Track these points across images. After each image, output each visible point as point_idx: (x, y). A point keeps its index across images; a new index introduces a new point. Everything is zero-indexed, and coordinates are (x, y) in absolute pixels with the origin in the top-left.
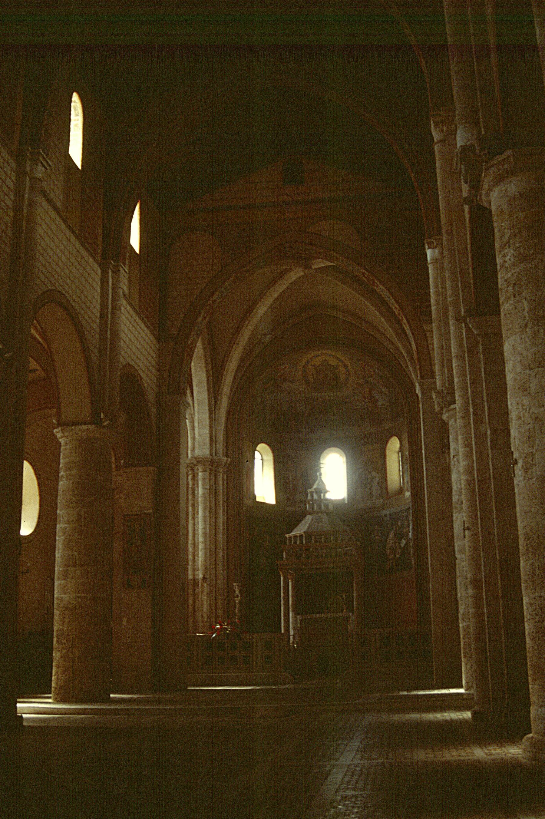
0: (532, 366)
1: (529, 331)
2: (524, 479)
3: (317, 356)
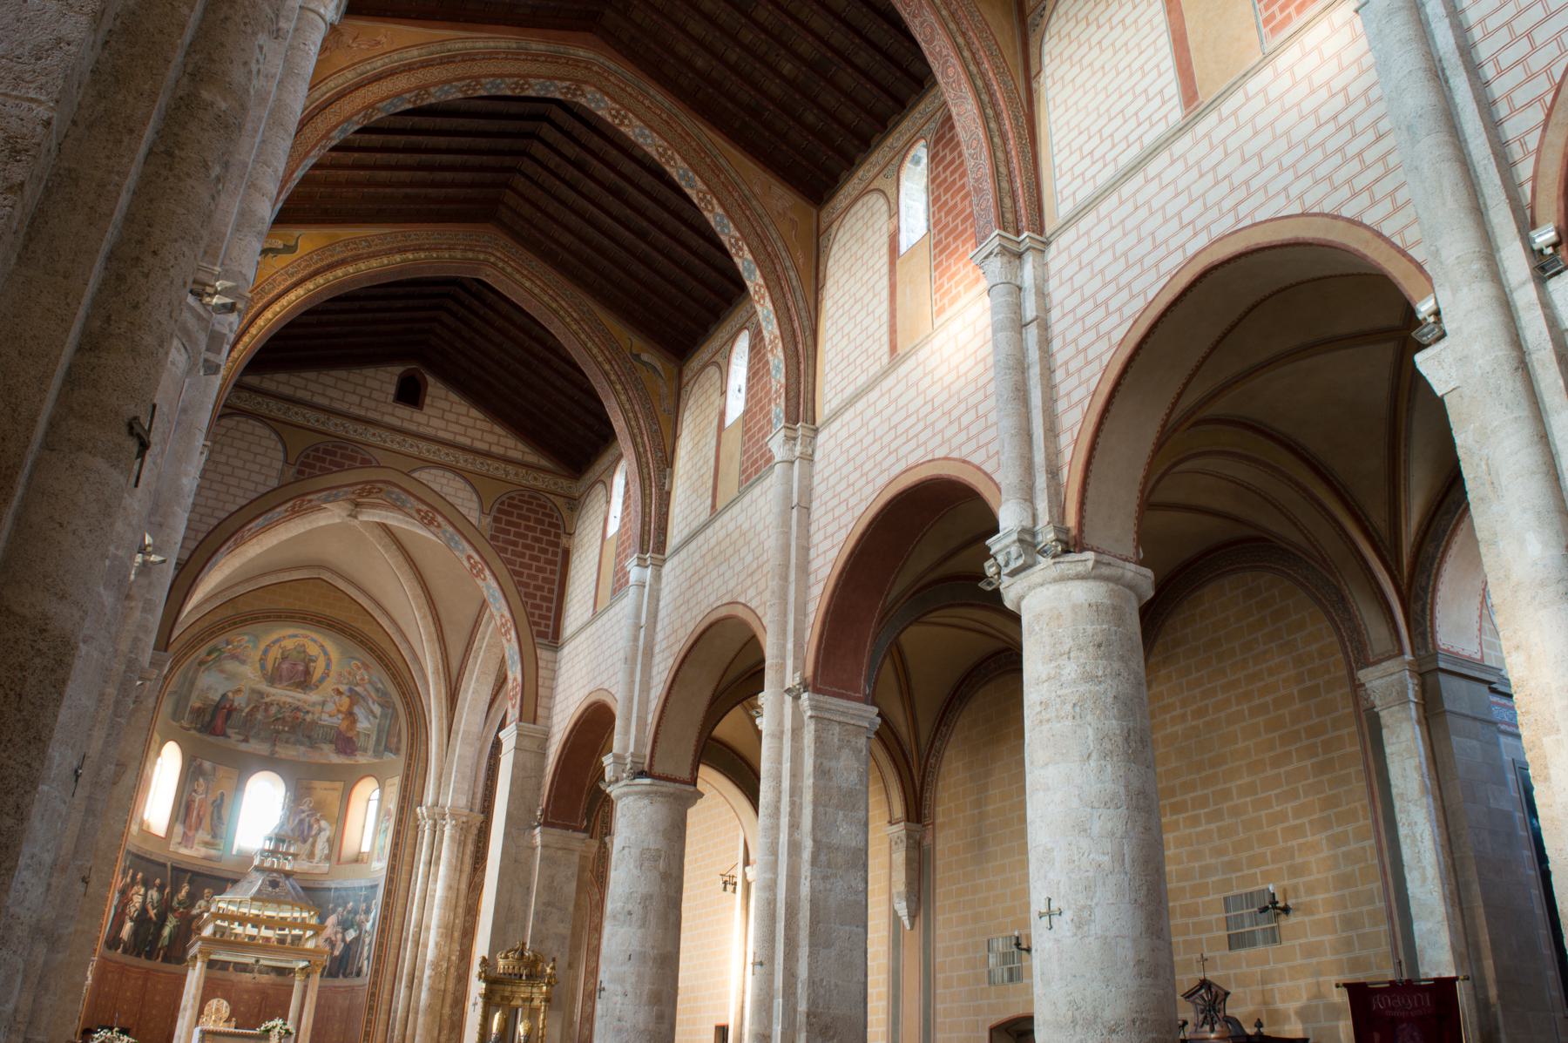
0: (1096, 804)
1: (1092, 763)
2: (1075, 935)
3: (295, 636)
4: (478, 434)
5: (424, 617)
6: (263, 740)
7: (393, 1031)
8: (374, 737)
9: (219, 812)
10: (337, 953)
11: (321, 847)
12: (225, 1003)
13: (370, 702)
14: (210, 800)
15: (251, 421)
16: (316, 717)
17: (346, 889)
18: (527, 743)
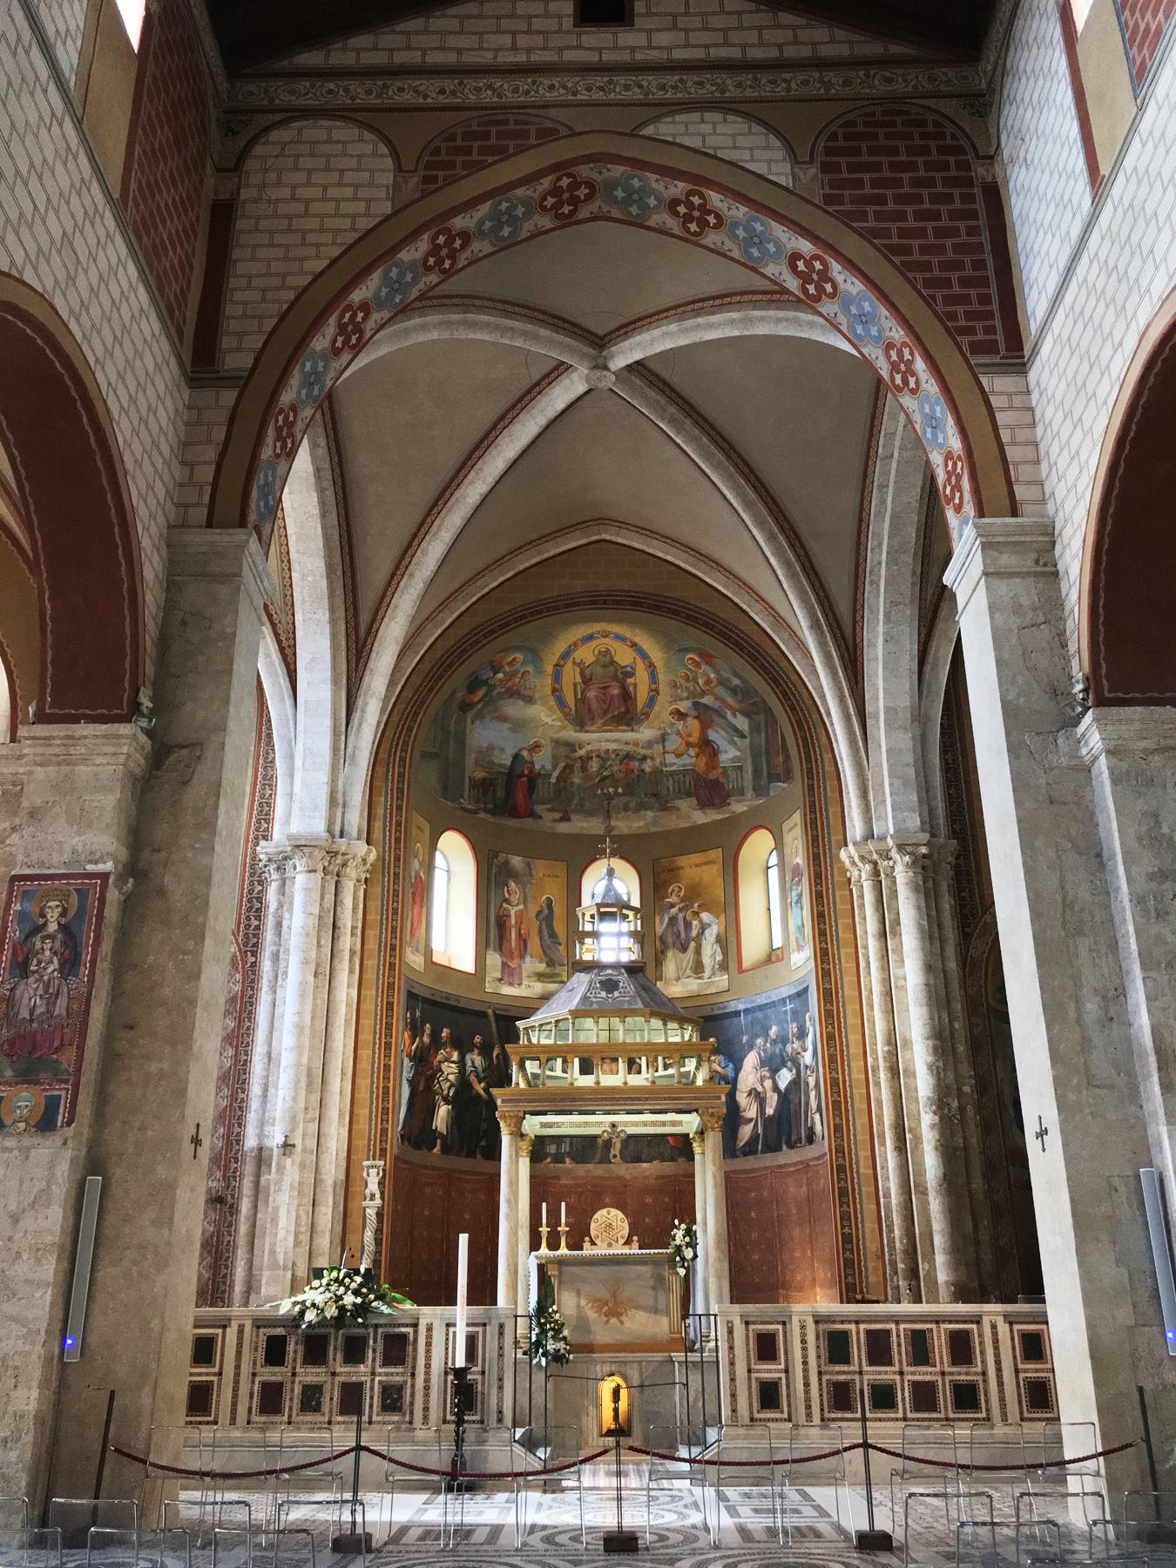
3: (590, 638)
4: (752, 37)
5: (771, 538)
6: (591, 813)
7: (891, 1230)
8: (749, 768)
9: (550, 927)
10: (770, 1111)
11: (710, 952)
12: (620, 1215)
13: (729, 715)
14: (533, 910)
15: (323, 123)
16: (658, 760)
17: (761, 1008)
18: (1007, 560)
